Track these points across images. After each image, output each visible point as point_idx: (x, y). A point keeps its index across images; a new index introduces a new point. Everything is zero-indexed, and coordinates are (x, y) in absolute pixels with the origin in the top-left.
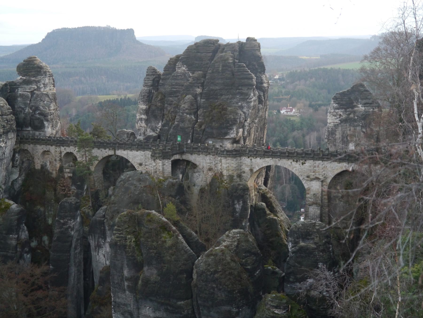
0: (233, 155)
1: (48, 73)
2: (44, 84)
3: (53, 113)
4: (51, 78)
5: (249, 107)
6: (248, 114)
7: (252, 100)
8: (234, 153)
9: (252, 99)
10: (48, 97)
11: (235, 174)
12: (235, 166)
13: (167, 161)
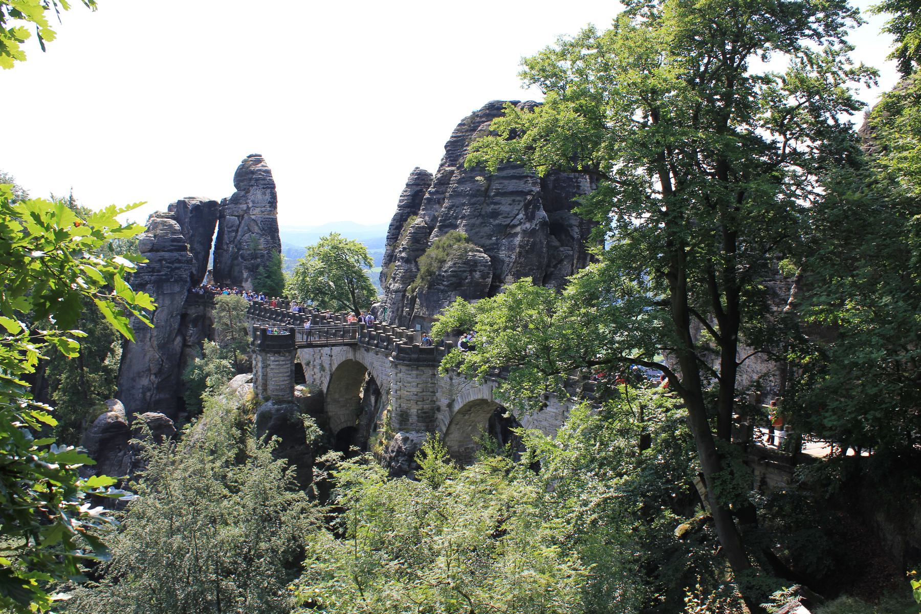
0: (410, 361)
2: (253, 202)
4: (269, 191)
5: (511, 249)
7: (518, 229)
8: (414, 356)
9: (515, 226)
10: (257, 225)
11: (414, 411)
12: (414, 390)
13: (272, 358)
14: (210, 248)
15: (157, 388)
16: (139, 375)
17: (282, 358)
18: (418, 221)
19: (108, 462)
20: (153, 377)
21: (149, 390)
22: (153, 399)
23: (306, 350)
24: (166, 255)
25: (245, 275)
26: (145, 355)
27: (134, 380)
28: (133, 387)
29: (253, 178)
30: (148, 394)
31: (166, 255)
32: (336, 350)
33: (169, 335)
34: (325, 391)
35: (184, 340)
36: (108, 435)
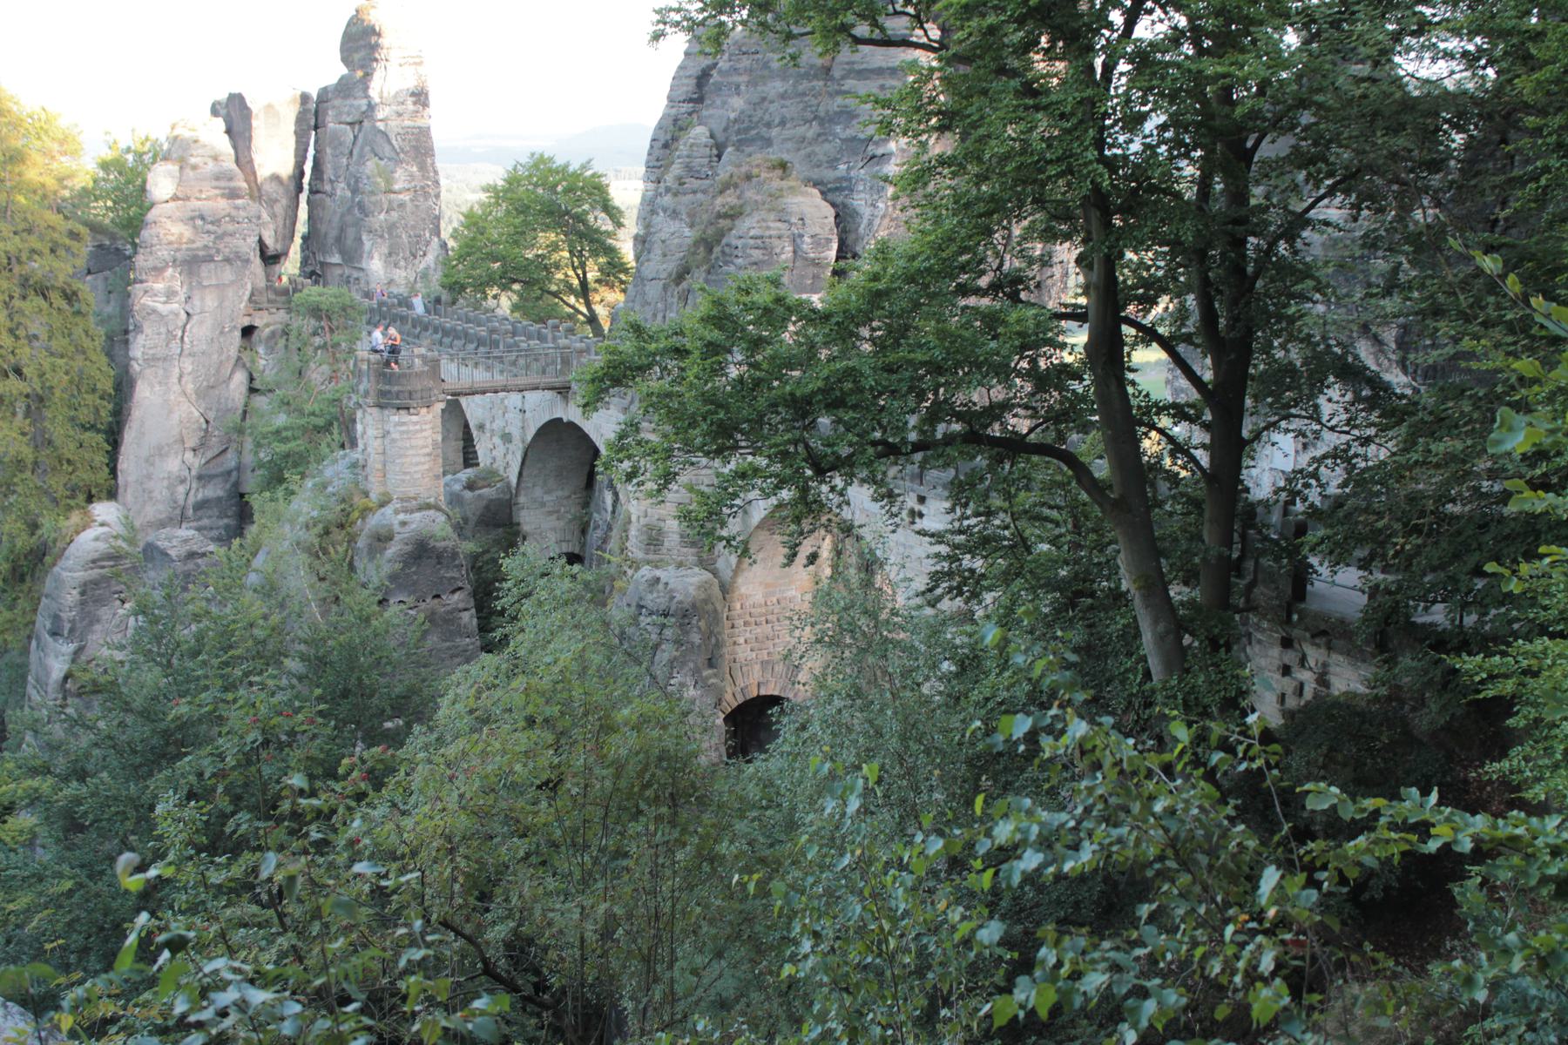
3: (402, 205)
6: (870, 223)
13: (396, 418)
14: (300, 189)
15: (200, 478)
16: (160, 452)
17: (414, 418)
18: (699, 133)
19: (98, 627)
20: (189, 455)
21: (183, 481)
22: (191, 500)
23: (477, 398)
25: (367, 245)
26: (171, 412)
27: (149, 461)
28: (149, 477)
29: (360, 43)
30: (181, 489)
32: (533, 397)
33: (218, 371)
34: (514, 480)
35: (252, 379)
36: (95, 573)
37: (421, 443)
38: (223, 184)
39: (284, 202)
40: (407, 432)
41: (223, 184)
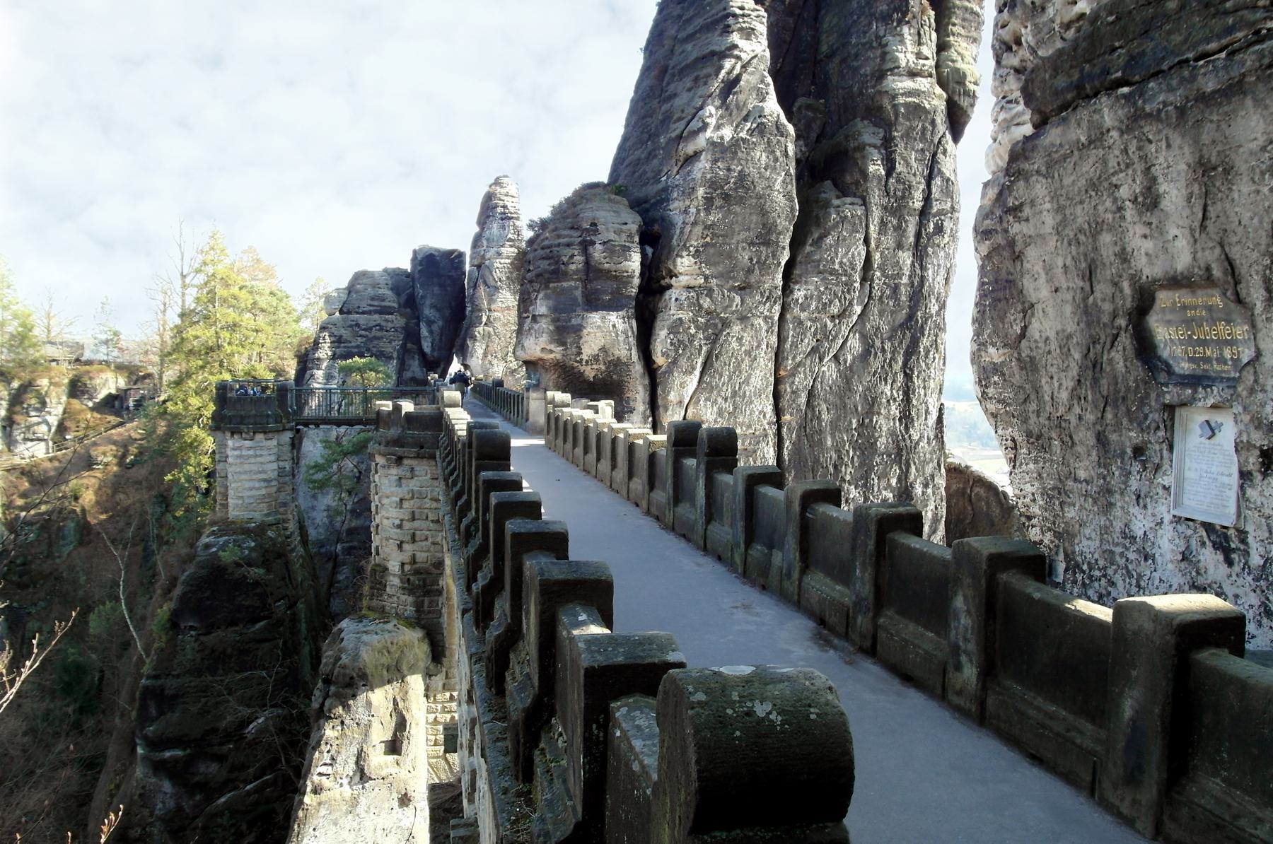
1: (500, 210)
2: (488, 240)
7: (701, 141)
17: (248, 443)
21: (339, 513)
22: (346, 527)
24: (362, 319)
28: (313, 508)
30: (339, 519)
31: (362, 319)
37: (255, 468)
38: (376, 303)
39: (440, 323)
40: (241, 456)
41: (376, 303)
